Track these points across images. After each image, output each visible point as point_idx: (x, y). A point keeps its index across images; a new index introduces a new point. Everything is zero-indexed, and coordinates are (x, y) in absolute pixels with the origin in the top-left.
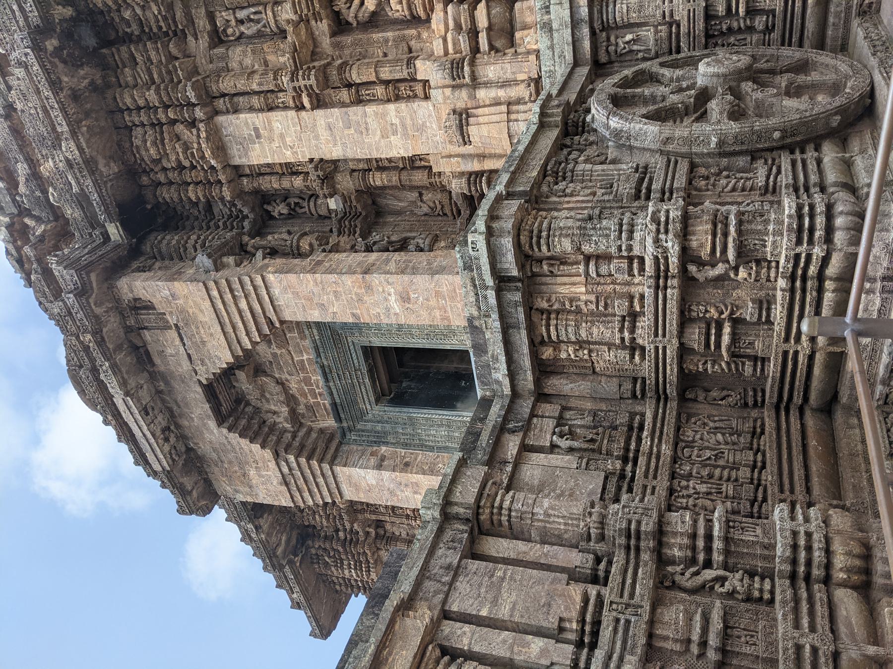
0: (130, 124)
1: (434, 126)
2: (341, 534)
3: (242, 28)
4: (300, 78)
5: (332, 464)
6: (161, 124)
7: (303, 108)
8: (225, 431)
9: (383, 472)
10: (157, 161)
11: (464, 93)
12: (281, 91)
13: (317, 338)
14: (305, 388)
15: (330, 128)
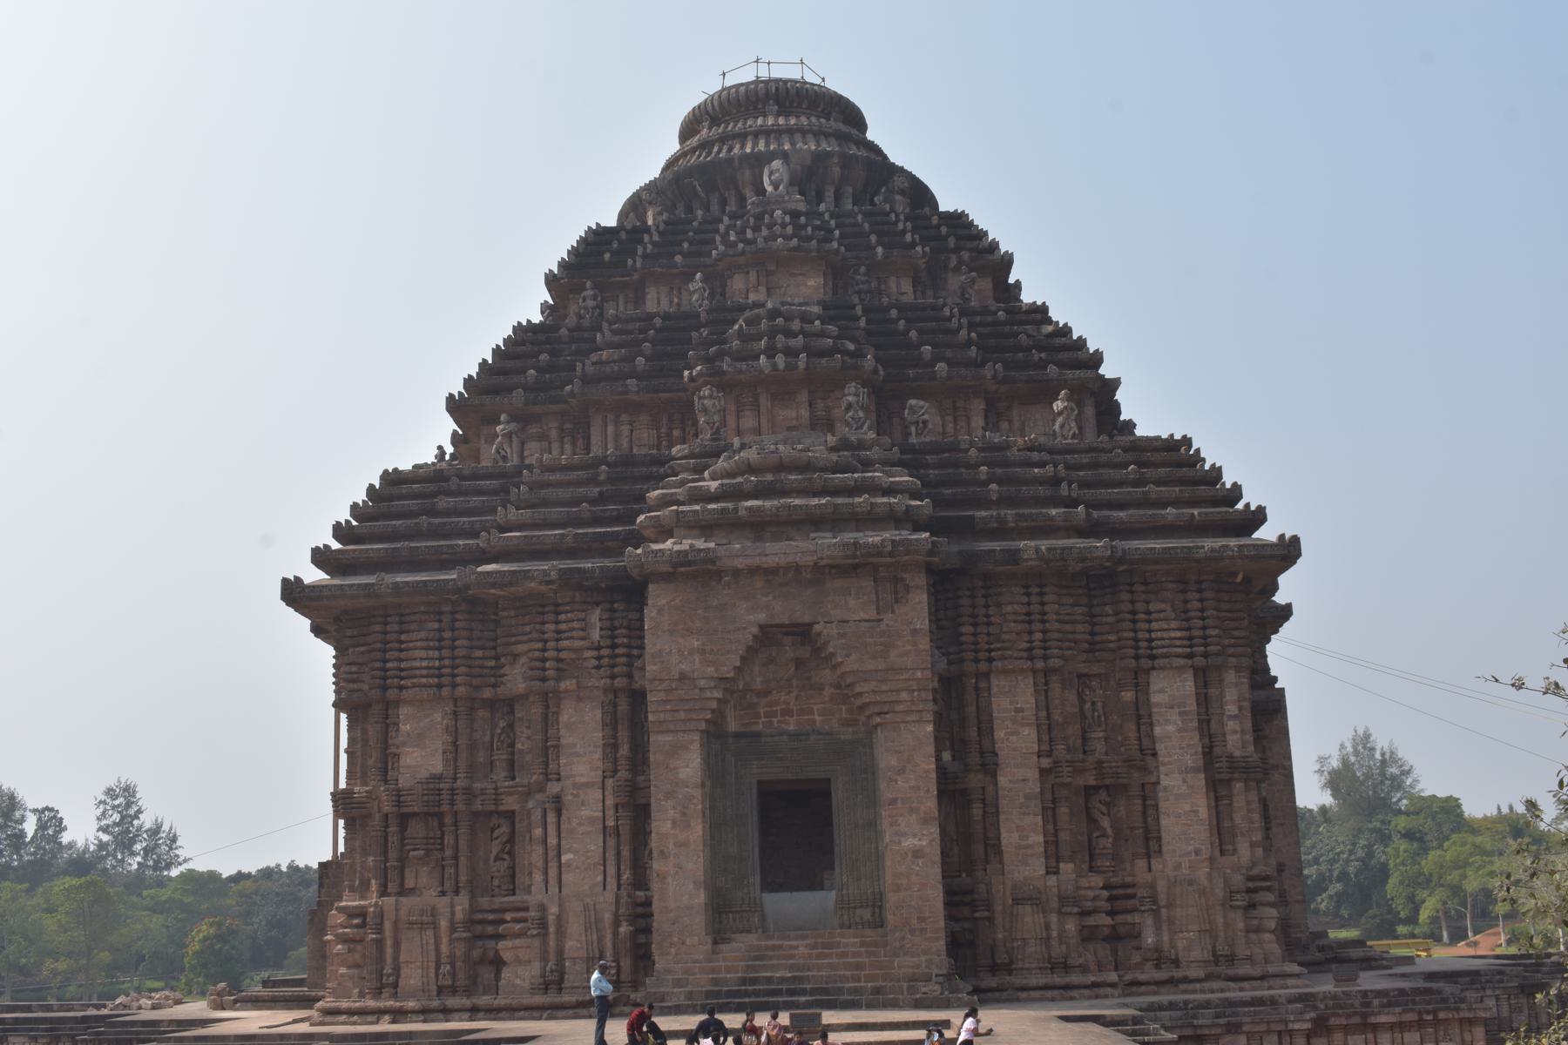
0: (1030, 590)
1: (1027, 873)
2: (479, 653)
3: (1090, 704)
4: (1070, 769)
5: (706, 733)
6: (1030, 622)
7: (1039, 757)
8: (755, 630)
9: (700, 790)
10: (999, 605)
11: (1055, 905)
12: (1051, 740)
13: (842, 737)
14: (779, 708)
15: (1024, 780)
